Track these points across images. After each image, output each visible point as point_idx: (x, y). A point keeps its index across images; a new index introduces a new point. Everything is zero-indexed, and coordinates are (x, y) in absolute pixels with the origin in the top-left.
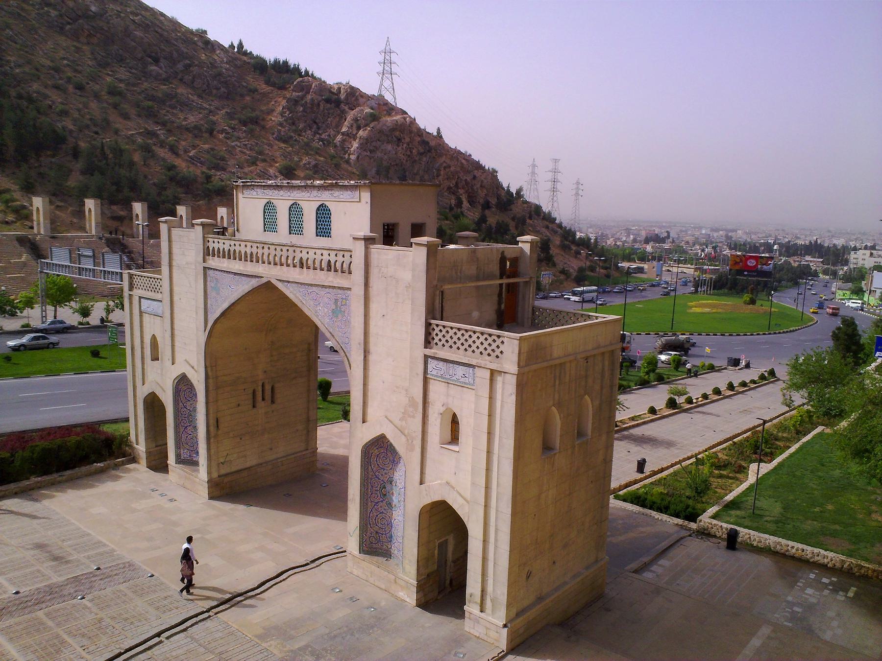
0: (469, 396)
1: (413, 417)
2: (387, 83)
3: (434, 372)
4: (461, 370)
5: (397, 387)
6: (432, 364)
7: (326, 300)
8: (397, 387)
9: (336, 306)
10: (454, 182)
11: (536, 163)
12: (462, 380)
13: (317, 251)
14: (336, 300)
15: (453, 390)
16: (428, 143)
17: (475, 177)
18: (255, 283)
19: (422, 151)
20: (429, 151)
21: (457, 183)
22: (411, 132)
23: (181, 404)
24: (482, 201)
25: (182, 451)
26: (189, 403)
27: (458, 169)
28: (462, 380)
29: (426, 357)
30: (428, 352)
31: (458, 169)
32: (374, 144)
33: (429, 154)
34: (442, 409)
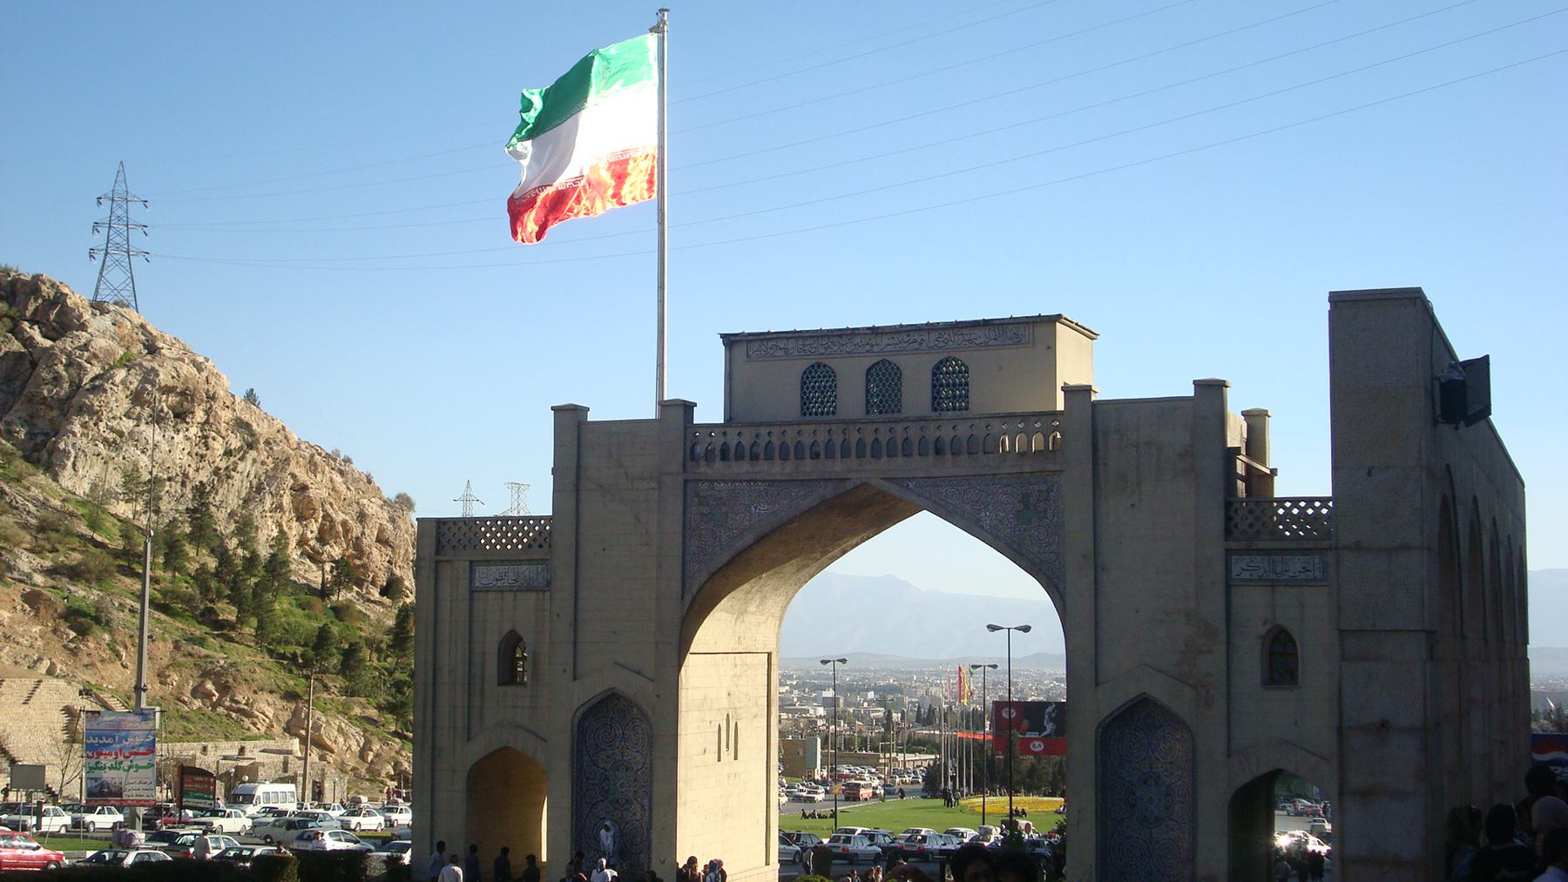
2: (116, 277)
3: (1245, 575)
4: (1296, 564)
6: (1239, 566)
10: (315, 526)
11: (475, 492)
16: (248, 426)
17: (362, 517)
18: (828, 491)
19: (235, 443)
20: (251, 446)
21: (321, 530)
22: (212, 398)
24: (383, 580)
27: (324, 493)
28: (1303, 576)
29: (1228, 552)
30: (1232, 545)
31: (324, 493)
32: (114, 423)
33: (253, 453)
34: (1263, 630)
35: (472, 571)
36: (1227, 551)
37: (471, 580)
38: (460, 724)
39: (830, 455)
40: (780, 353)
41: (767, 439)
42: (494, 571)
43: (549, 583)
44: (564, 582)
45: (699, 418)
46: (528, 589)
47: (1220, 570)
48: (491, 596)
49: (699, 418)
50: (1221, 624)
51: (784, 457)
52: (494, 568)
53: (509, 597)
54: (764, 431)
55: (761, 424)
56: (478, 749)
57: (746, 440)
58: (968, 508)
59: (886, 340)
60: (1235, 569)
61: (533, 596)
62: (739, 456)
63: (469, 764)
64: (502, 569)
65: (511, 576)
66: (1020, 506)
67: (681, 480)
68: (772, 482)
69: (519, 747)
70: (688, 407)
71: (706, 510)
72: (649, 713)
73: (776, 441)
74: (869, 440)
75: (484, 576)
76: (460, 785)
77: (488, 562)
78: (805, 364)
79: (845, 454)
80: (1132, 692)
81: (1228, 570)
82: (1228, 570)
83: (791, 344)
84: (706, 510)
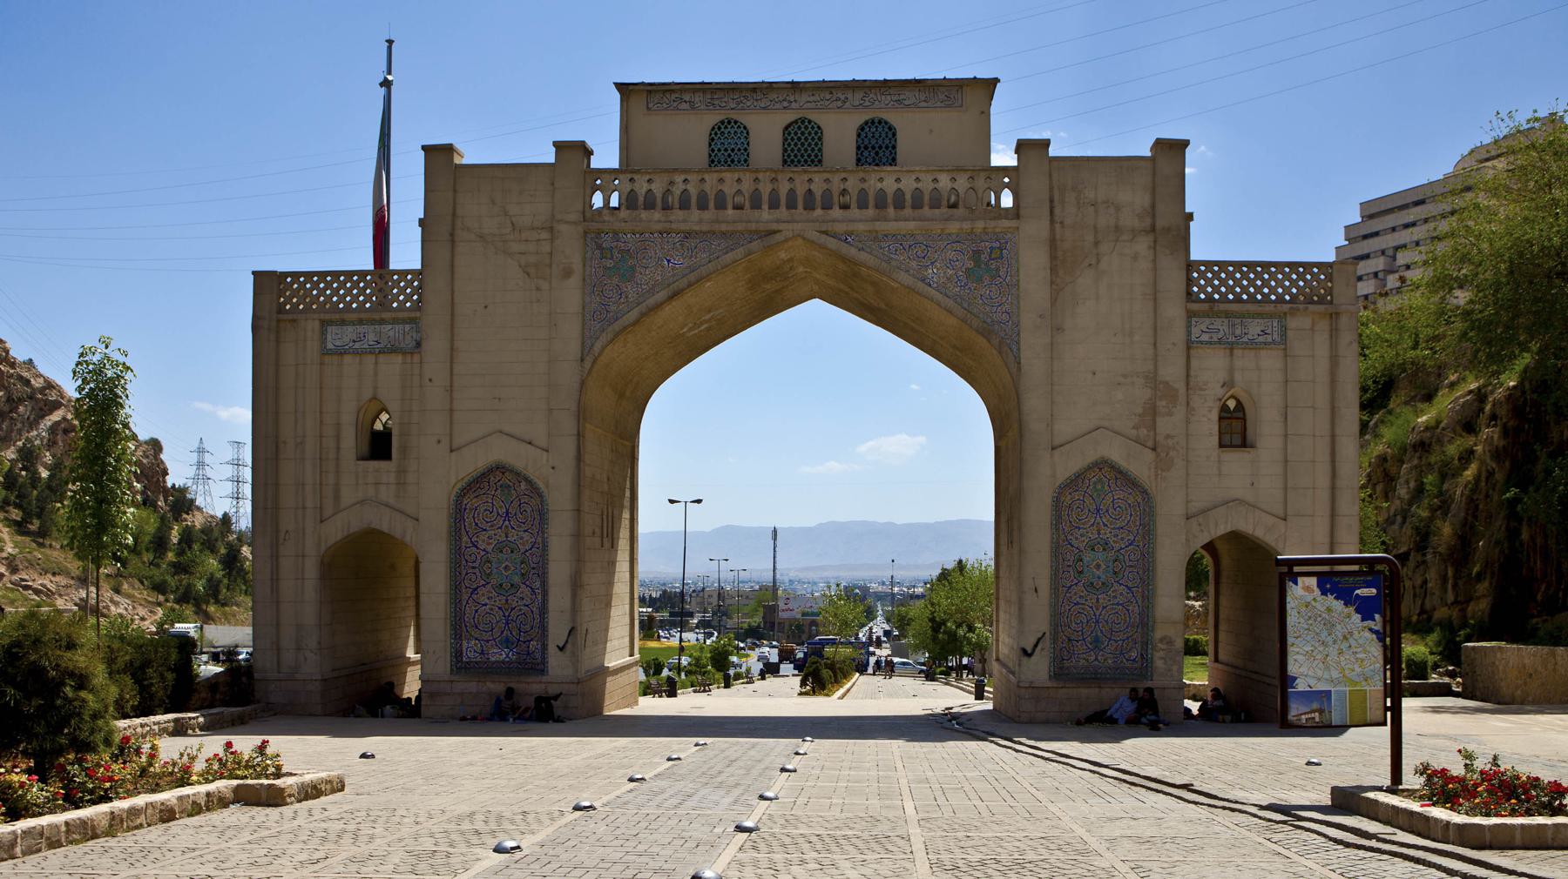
0: (1270, 361)
1: (1170, 414)
3: (1205, 337)
4: (1254, 328)
5: (1125, 376)
7: (951, 255)
8: (1125, 376)
9: (977, 261)
12: (1261, 339)
13: (922, 176)
14: (977, 253)
15: (1244, 360)
23: (465, 539)
25: (465, 643)
26: (484, 536)
28: (1261, 339)
29: (1190, 315)
35: (323, 333)
36: (1188, 311)
37: (324, 341)
38: (309, 504)
39: (756, 205)
40: (684, 106)
41: (682, 187)
42: (349, 332)
43: (419, 344)
44: (435, 344)
45: (596, 162)
46: (393, 350)
47: (1179, 334)
48: (348, 359)
49: (596, 162)
50: (1182, 390)
51: (703, 206)
52: (350, 329)
53: (370, 359)
54: (679, 178)
55: (675, 170)
56: (335, 531)
57: (658, 188)
58: (914, 264)
59: (804, 98)
60: (1195, 332)
61: (399, 358)
62: (650, 205)
63: (323, 548)
64: (361, 329)
65: (371, 337)
66: (970, 264)
67: (580, 229)
68: (688, 235)
69: (385, 528)
70: (584, 150)
71: (610, 263)
72: (541, 485)
73: (693, 189)
74: (801, 191)
75: (339, 336)
76: (311, 570)
77: (343, 323)
78: (713, 118)
79: (774, 205)
80: (1091, 456)
81: (1189, 333)
82: (1189, 333)
83: (698, 98)
84: (610, 263)
